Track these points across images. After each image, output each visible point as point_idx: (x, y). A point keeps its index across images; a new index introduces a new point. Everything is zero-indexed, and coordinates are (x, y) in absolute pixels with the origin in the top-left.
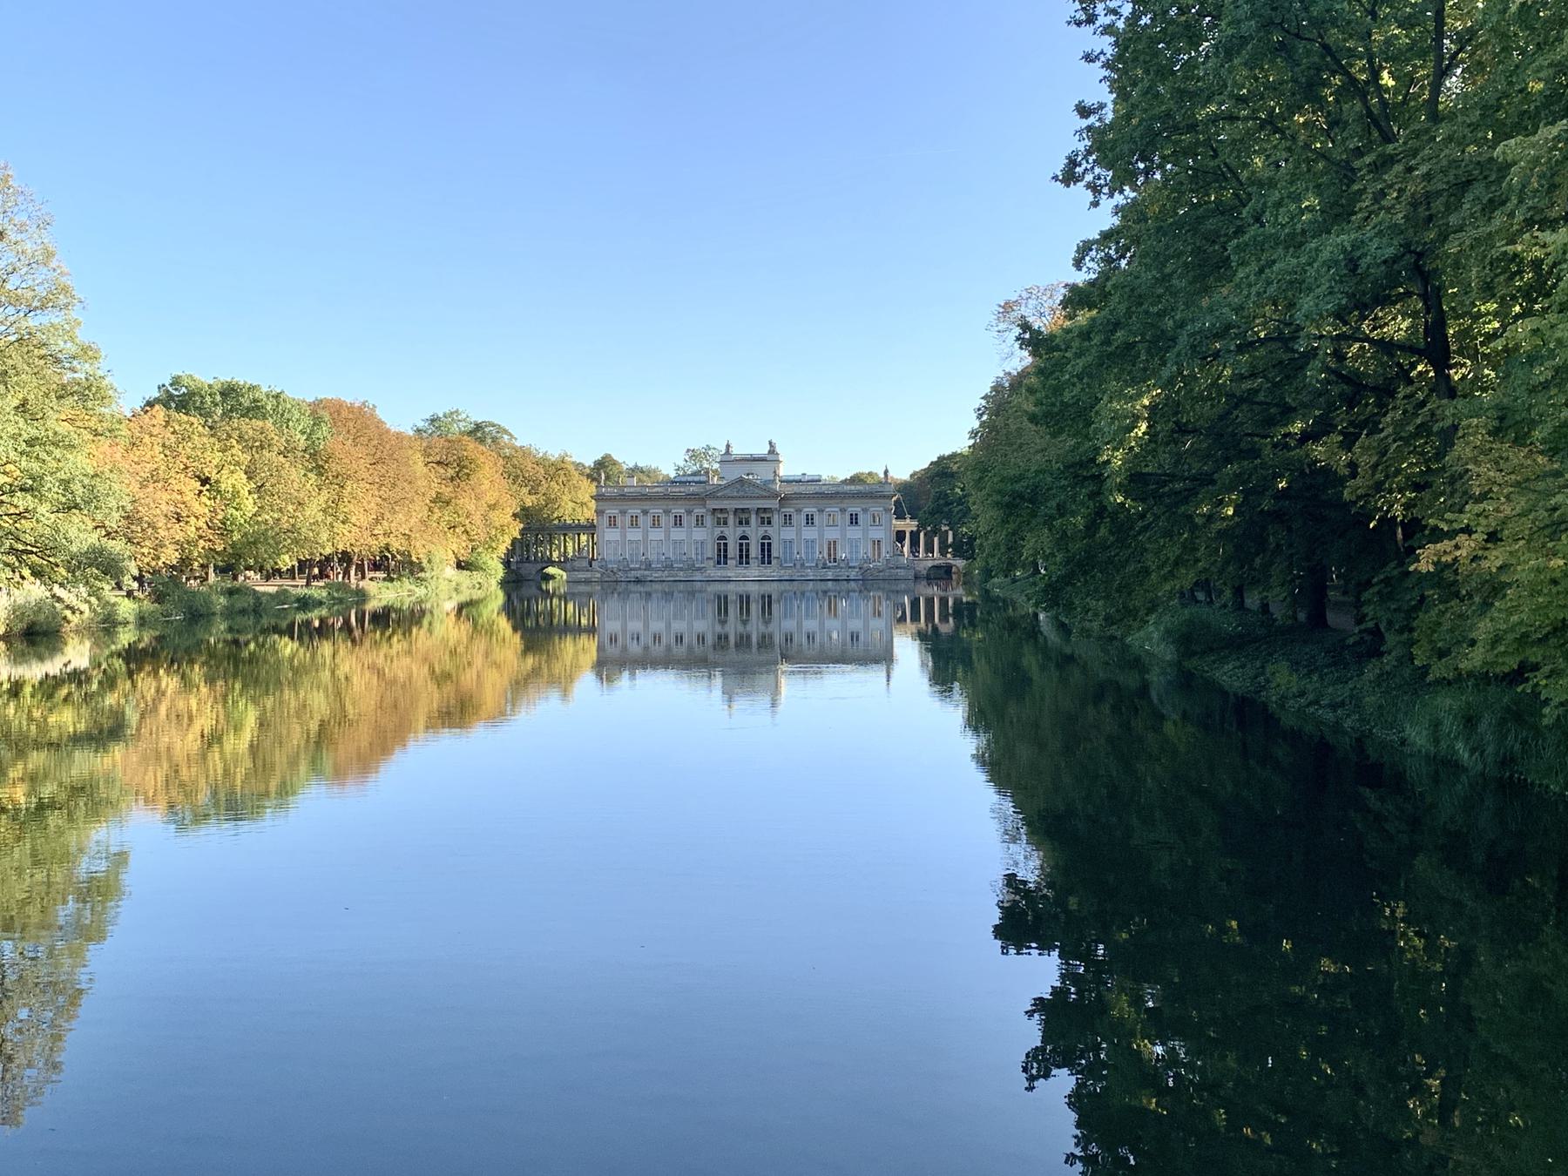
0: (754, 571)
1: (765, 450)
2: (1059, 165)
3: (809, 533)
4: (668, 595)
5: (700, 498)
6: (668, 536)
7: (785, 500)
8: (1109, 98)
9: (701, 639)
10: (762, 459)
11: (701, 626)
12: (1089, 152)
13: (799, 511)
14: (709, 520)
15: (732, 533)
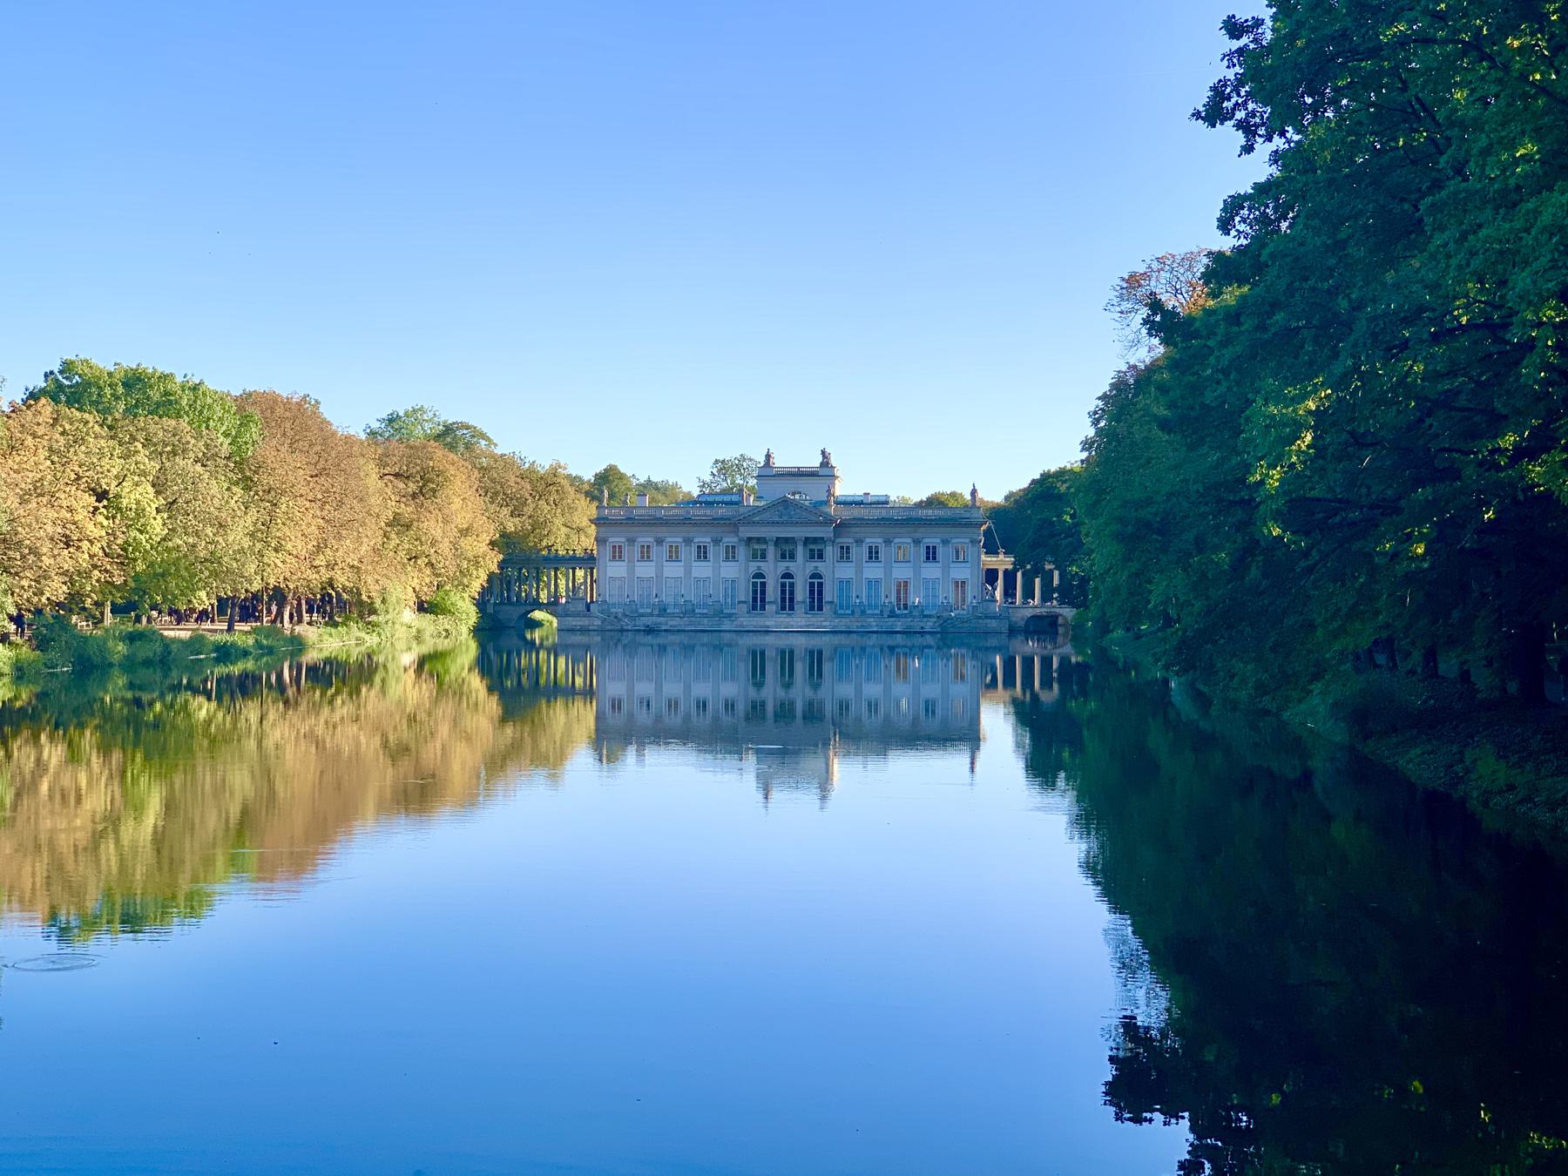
0: (799, 620)
1: (815, 462)
2: (1201, 98)
3: (873, 571)
4: (688, 649)
5: (732, 524)
6: (688, 571)
7: (842, 527)
8: (1267, 13)
9: (730, 706)
10: (811, 474)
11: (729, 690)
12: (1240, 81)
13: (859, 542)
14: (742, 552)
15: (772, 569)
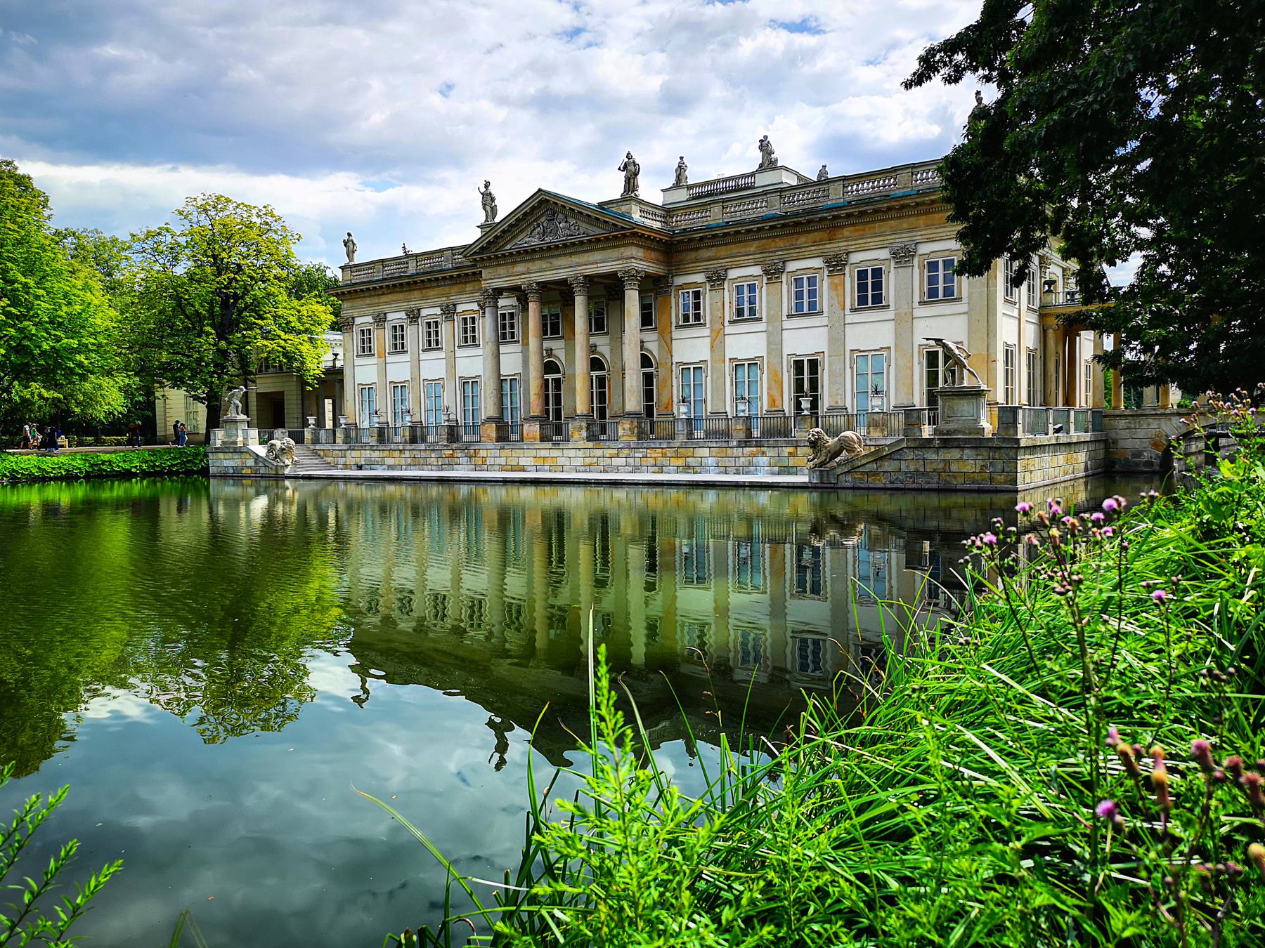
3: (746, 343)
6: (452, 366)
13: (717, 279)
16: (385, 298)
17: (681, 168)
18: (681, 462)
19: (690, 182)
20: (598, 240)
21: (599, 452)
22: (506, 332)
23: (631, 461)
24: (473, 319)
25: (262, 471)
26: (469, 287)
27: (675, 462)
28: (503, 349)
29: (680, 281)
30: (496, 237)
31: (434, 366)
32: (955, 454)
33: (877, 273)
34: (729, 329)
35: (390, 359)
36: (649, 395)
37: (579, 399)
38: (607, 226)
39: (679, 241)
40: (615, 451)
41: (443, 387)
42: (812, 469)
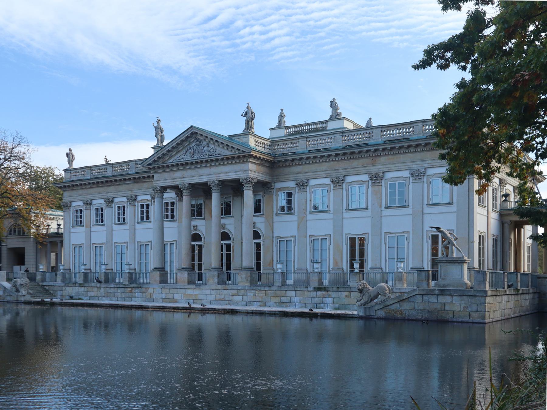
1: (326, 114)
13: (302, 185)
16: (92, 190)
17: (281, 117)
18: (277, 300)
19: (287, 124)
20: (228, 159)
21: (225, 292)
22: (169, 212)
23: (246, 298)
24: (147, 205)
25: (8, 298)
26: (146, 185)
27: (274, 299)
28: (166, 224)
29: (278, 185)
30: (164, 154)
31: (121, 234)
32: (448, 299)
33: (401, 185)
34: (310, 216)
35: (93, 229)
36: (258, 257)
37: (212, 257)
38: (236, 151)
39: (279, 161)
40: (236, 292)
41: (127, 247)
42: (360, 306)
